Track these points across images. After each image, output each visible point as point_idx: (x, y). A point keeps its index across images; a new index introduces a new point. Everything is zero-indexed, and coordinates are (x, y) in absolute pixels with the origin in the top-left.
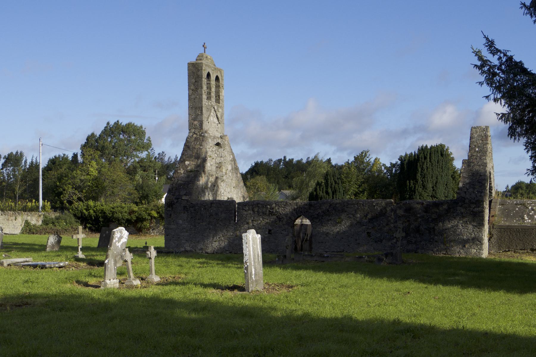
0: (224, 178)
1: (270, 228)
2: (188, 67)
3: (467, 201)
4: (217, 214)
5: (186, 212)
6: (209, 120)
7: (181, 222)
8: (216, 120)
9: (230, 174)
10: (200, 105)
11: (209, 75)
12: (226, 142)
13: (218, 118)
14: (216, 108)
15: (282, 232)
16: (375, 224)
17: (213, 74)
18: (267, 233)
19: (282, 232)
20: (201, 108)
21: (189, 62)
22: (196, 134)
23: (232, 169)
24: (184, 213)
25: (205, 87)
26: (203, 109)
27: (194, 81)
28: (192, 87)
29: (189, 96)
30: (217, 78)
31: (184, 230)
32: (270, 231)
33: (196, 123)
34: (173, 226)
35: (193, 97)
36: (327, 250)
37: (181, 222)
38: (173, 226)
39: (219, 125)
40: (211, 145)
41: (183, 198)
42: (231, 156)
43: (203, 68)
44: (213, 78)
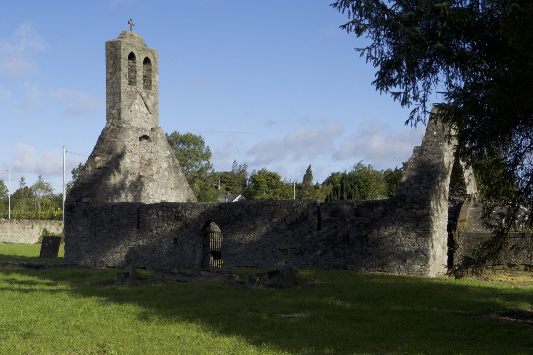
0: (155, 177)
1: (176, 237)
2: (106, 46)
3: (408, 200)
5: (86, 218)
7: (80, 229)
8: (144, 109)
9: (166, 173)
10: (118, 91)
11: (132, 56)
12: (159, 135)
13: (147, 107)
14: (144, 95)
15: (189, 242)
16: (295, 231)
17: (139, 55)
18: (172, 242)
19: (189, 242)
20: (119, 94)
21: (107, 41)
22: (114, 125)
23: (169, 167)
24: (84, 218)
26: (122, 95)
27: (112, 62)
28: (110, 70)
29: (107, 80)
30: (147, 61)
31: (85, 239)
32: (175, 239)
33: (114, 111)
35: (111, 81)
36: (239, 265)
37: (80, 229)
39: (150, 115)
40: (132, 137)
41: (84, 201)
43: (122, 47)
44: (140, 59)
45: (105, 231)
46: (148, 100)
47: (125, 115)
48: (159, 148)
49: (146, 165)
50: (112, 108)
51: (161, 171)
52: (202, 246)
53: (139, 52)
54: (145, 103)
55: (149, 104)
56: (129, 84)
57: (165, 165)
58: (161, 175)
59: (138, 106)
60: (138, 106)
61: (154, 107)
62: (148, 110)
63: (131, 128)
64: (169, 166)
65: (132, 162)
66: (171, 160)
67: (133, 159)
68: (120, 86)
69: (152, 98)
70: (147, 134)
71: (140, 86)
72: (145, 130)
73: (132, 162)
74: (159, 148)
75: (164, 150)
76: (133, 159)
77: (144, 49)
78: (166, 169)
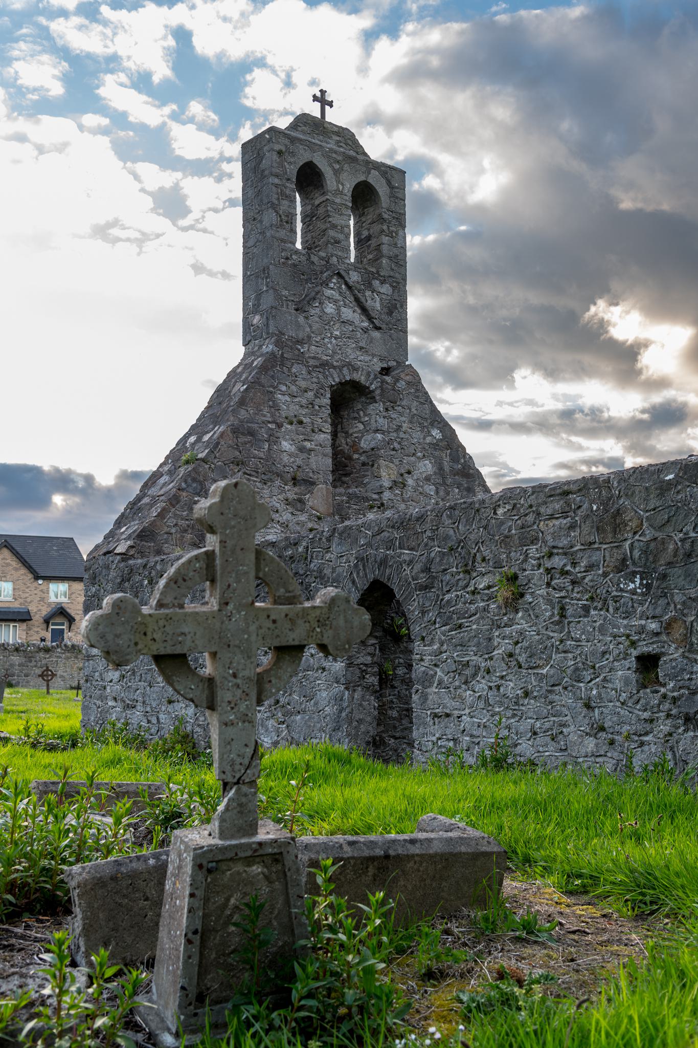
0: (387, 495)
9: (430, 489)
12: (401, 384)
17: (336, 173)
33: (256, 319)
35: (251, 243)
39: (376, 334)
40: (303, 384)
44: (340, 185)
46: (368, 293)
49: (364, 464)
51: (410, 482)
52: (373, 680)
53: (337, 166)
54: (357, 300)
55: (375, 304)
57: (426, 467)
61: (390, 313)
62: (370, 319)
64: (441, 469)
65: (302, 449)
67: (308, 445)
69: (386, 289)
73: (302, 449)
75: (423, 427)
76: (308, 445)
78: (427, 479)
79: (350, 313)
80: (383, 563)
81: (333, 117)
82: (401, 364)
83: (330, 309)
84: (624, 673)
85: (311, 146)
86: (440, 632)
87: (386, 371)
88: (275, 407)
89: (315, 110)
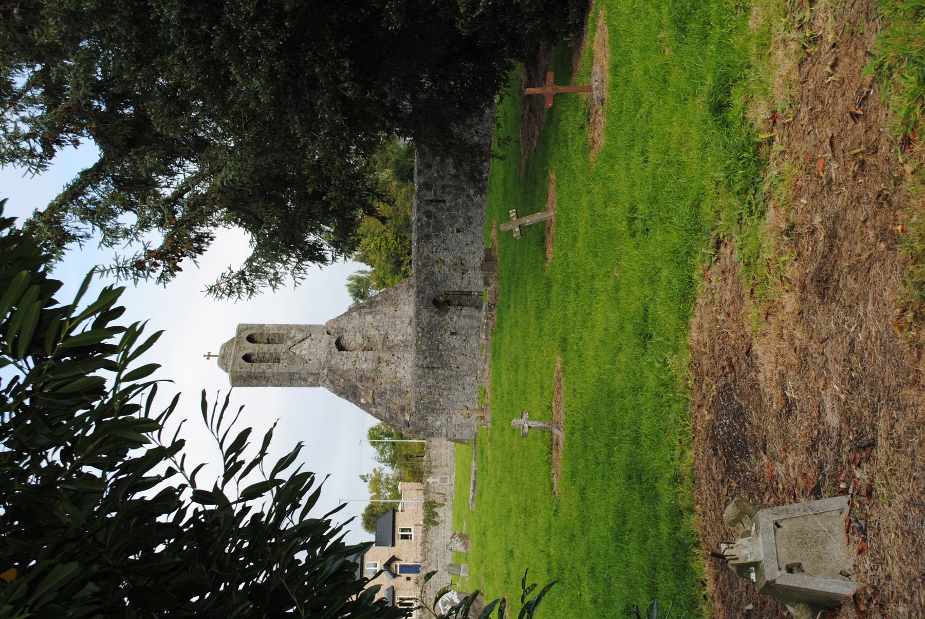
0: (382, 332)
1: (449, 333)
4: (429, 388)
6: (307, 358)
7: (438, 423)
9: (378, 317)
11: (247, 358)
12: (335, 326)
13: (303, 340)
14: (290, 343)
17: (245, 349)
25: (263, 366)
27: (255, 382)
28: (264, 383)
30: (251, 339)
32: (452, 333)
33: (310, 380)
34: (444, 431)
35: (276, 382)
37: (438, 423)
38: (444, 431)
39: (313, 336)
40: (339, 361)
42: (354, 314)
44: (250, 348)
45: (441, 400)
47: (313, 366)
48: (350, 326)
50: (306, 380)
51: (376, 324)
55: (300, 336)
56: (279, 362)
57: (369, 318)
58: (380, 325)
59: (303, 350)
60: (303, 350)
63: (328, 361)
65: (366, 361)
66: (364, 311)
68: (281, 373)
69: (293, 332)
70: (334, 340)
71: (280, 348)
72: (330, 343)
74: (350, 326)
77: (238, 342)
79: (306, 344)
80: (428, 299)
81: (216, 351)
82: (325, 327)
83: (304, 352)
84: (460, 236)
85: (235, 358)
86: (448, 283)
87: (328, 333)
88: (349, 370)
89: (215, 360)
